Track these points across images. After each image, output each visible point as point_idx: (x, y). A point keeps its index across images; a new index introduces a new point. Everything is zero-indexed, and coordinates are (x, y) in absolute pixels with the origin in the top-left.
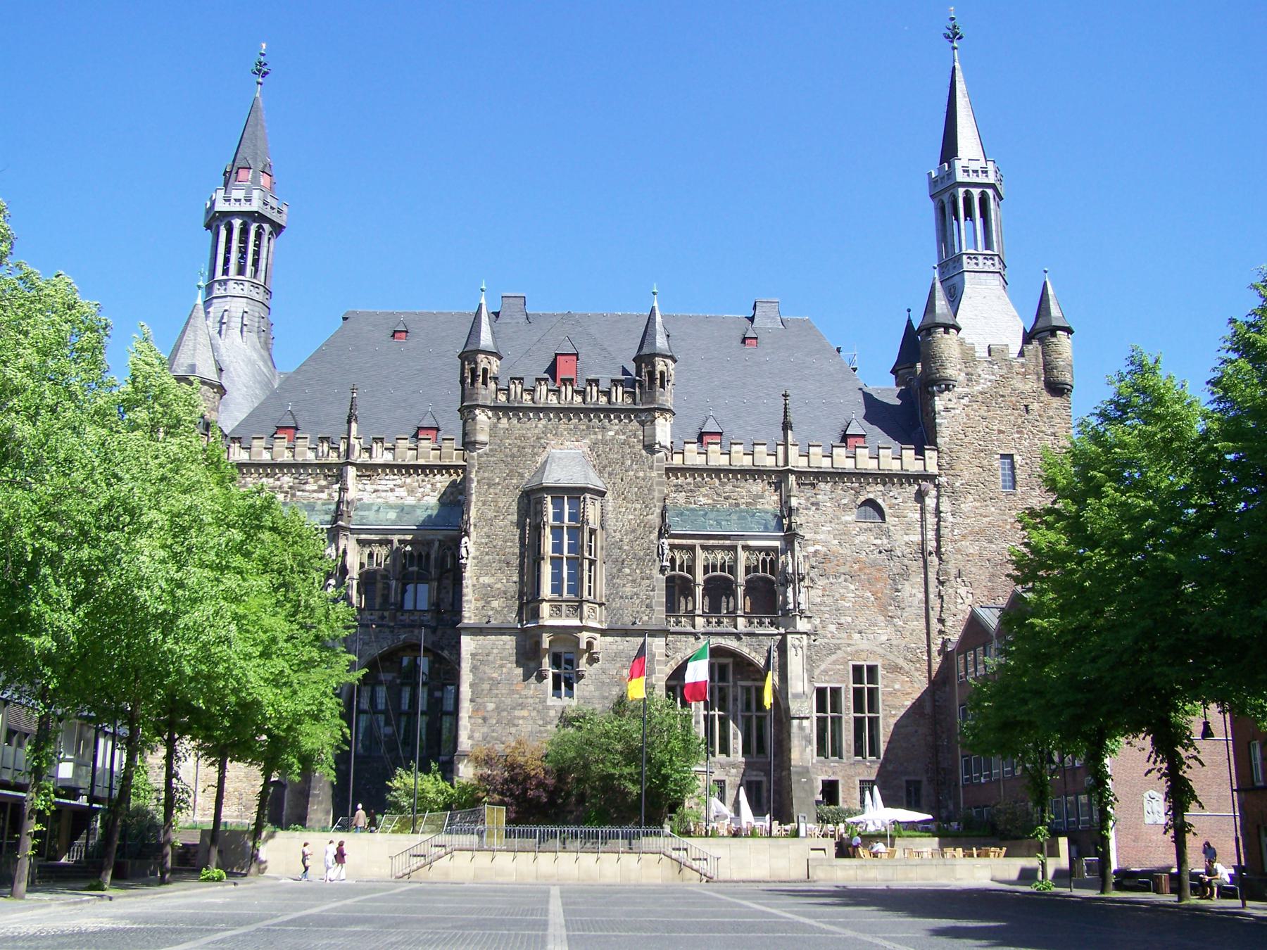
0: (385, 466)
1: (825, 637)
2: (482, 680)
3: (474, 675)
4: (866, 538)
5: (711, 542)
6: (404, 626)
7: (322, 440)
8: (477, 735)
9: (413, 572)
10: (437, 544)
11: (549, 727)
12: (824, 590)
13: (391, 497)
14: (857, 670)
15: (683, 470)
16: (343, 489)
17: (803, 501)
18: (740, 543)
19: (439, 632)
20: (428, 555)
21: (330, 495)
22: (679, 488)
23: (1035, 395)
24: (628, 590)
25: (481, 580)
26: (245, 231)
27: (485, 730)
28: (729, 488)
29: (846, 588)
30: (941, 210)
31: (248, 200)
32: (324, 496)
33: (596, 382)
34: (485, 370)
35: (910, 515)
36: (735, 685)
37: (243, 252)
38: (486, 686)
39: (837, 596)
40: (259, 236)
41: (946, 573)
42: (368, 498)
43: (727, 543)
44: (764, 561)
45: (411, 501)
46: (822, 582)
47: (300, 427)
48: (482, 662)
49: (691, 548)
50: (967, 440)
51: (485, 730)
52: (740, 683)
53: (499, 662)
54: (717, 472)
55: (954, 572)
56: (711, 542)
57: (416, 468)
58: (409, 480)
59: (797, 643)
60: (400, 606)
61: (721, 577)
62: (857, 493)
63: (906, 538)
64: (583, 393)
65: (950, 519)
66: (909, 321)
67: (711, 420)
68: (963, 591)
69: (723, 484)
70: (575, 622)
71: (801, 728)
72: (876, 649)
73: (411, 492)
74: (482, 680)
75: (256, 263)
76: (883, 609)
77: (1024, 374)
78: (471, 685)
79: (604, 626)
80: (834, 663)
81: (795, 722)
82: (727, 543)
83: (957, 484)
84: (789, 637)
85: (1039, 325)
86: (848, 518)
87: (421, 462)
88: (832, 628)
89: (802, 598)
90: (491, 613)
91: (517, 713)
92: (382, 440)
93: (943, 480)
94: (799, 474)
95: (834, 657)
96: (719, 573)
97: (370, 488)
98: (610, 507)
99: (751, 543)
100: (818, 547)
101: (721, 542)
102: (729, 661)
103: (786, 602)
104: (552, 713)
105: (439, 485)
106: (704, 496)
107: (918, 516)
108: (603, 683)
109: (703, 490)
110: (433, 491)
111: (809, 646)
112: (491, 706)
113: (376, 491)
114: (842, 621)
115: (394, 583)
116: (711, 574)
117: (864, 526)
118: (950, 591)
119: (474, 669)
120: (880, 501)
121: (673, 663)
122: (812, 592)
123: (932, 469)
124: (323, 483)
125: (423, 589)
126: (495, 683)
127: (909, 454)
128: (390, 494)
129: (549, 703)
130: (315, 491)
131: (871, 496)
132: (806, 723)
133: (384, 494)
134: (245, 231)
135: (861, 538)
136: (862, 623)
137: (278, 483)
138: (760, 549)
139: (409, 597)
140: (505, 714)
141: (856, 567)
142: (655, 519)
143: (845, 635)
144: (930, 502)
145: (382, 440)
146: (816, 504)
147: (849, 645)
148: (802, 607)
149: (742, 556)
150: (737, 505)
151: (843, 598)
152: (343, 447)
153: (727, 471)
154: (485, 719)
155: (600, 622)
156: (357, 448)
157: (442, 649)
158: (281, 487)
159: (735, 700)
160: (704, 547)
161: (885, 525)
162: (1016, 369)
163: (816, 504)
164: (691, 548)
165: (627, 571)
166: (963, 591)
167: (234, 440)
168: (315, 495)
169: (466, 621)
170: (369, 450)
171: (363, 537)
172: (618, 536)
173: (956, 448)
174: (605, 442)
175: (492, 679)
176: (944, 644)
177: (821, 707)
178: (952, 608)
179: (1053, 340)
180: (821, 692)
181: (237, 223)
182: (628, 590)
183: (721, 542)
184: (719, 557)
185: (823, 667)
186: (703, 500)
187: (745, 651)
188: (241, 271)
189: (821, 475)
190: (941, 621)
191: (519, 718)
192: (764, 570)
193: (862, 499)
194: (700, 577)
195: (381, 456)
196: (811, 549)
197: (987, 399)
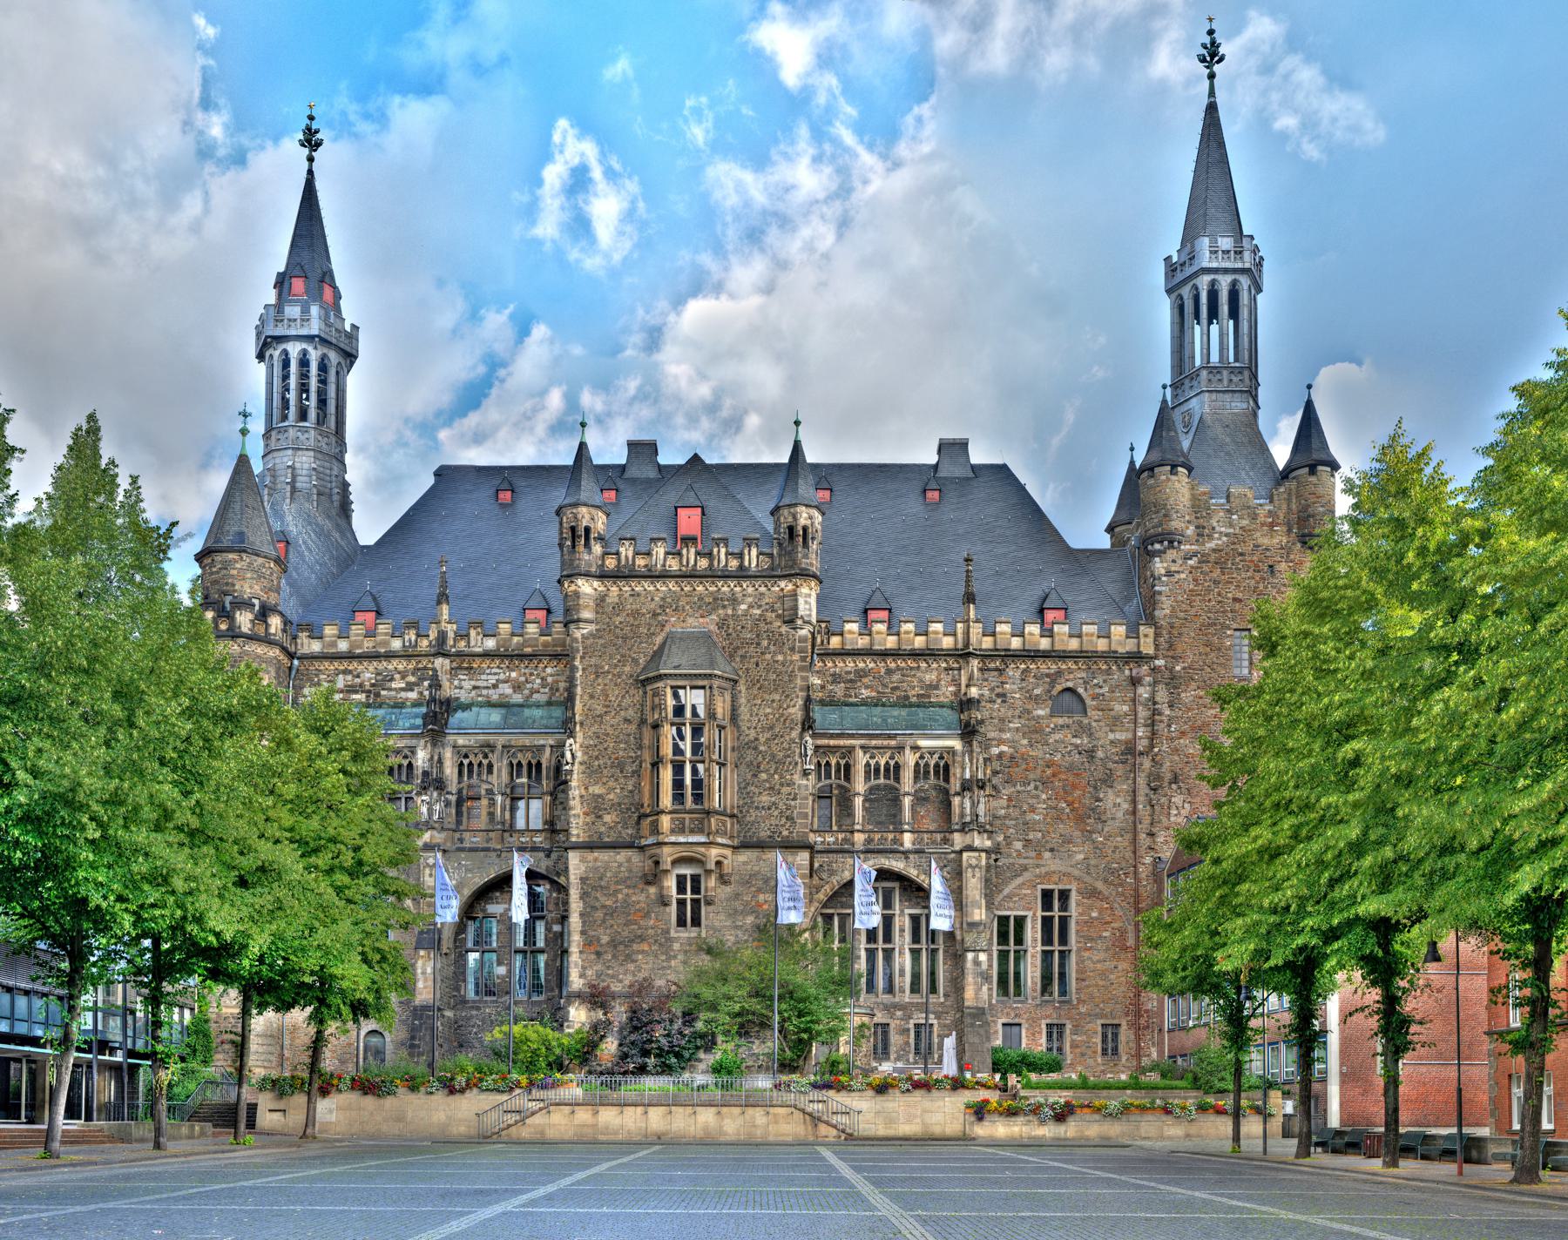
0: (486, 655)
1: (1009, 856)
2: (594, 908)
3: (585, 903)
4: (1063, 739)
5: (874, 742)
7: (413, 625)
8: (589, 972)
9: (522, 785)
10: (548, 750)
11: (673, 963)
12: (1010, 799)
13: (494, 696)
14: (1047, 896)
15: (843, 653)
16: (436, 684)
17: (986, 693)
18: (910, 742)
19: (554, 856)
20: (539, 764)
21: (421, 693)
23: (1286, 551)
25: (591, 790)
27: (599, 967)
28: (896, 677)
29: (1038, 797)
30: (1180, 309)
31: (305, 319)
32: (413, 695)
35: (1117, 707)
36: (902, 911)
38: (599, 915)
39: (1025, 807)
41: (1159, 778)
42: (464, 696)
43: (893, 743)
44: (937, 766)
45: (517, 698)
46: (1006, 791)
47: (384, 611)
48: (594, 888)
49: (851, 750)
50: (1193, 612)
51: (599, 967)
52: (907, 911)
53: (612, 888)
55: (1168, 776)
57: (521, 657)
58: (514, 675)
59: (974, 862)
61: (877, 787)
62: (1053, 683)
63: (1111, 736)
65: (1167, 712)
66: (1132, 463)
67: (878, 594)
68: (1177, 800)
70: (703, 839)
71: (977, 963)
72: (1070, 870)
73: (517, 687)
74: (594, 908)
76: (1080, 819)
77: (1272, 525)
78: (582, 915)
79: (736, 843)
80: (1020, 887)
81: (970, 956)
82: (893, 743)
83: (1178, 668)
84: (965, 855)
85: (1294, 465)
86: (1041, 712)
87: (528, 650)
88: (1018, 845)
89: (981, 809)
90: (603, 829)
91: (635, 947)
92: (481, 624)
93: (1157, 662)
94: (985, 656)
95: (1019, 880)
96: (882, 781)
97: (467, 685)
99: (923, 743)
100: (1004, 748)
101: (886, 743)
102: (896, 885)
103: (962, 815)
104: (676, 946)
105: (550, 679)
106: (867, 687)
107: (1126, 708)
108: (736, 911)
109: (865, 680)
110: (544, 686)
111: (988, 867)
112: (605, 939)
113: (475, 688)
114: (1031, 837)
115: (499, 799)
116: (873, 782)
117: (1060, 721)
118: (1163, 800)
119: (584, 896)
120: (1081, 690)
121: (827, 887)
122: (994, 803)
123: (1148, 649)
124: (412, 679)
125: (536, 805)
126: (611, 912)
127: (1118, 631)
128: (491, 692)
129: (673, 934)
130: (402, 689)
131: (1070, 684)
132: (983, 957)
133: (485, 692)
135: (1057, 736)
136: (1054, 839)
137: (357, 681)
138: (932, 754)
139: (520, 814)
140: (621, 947)
141: (1049, 772)
143: (1033, 854)
144: (1144, 692)
145: (481, 624)
146: (1002, 695)
147: (1038, 866)
148: (982, 819)
150: (907, 698)
151: (1033, 810)
152: (433, 635)
154: (598, 954)
155: (732, 837)
156: (451, 635)
157: (558, 874)
158: (361, 685)
159: (902, 930)
160: (862, 747)
161: (1086, 721)
162: (1261, 519)
163: (1002, 695)
164: (851, 750)
165: (764, 776)
166: (1177, 800)
167: (300, 627)
168: (403, 694)
169: (574, 839)
170: (468, 635)
171: (461, 741)
173: (1177, 623)
175: (604, 906)
176: (1158, 860)
177: (1003, 937)
178: (1164, 820)
179: (1313, 479)
180: (1003, 921)
183: (886, 743)
184: (883, 763)
185: (1006, 891)
186: (865, 693)
187: (913, 873)
189: (1009, 656)
190: (1151, 835)
191: (639, 952)
192: (937, 773)
193: (1059, 688)
194: (860, 785)
196: (995, 751)
197: (1220, 560)
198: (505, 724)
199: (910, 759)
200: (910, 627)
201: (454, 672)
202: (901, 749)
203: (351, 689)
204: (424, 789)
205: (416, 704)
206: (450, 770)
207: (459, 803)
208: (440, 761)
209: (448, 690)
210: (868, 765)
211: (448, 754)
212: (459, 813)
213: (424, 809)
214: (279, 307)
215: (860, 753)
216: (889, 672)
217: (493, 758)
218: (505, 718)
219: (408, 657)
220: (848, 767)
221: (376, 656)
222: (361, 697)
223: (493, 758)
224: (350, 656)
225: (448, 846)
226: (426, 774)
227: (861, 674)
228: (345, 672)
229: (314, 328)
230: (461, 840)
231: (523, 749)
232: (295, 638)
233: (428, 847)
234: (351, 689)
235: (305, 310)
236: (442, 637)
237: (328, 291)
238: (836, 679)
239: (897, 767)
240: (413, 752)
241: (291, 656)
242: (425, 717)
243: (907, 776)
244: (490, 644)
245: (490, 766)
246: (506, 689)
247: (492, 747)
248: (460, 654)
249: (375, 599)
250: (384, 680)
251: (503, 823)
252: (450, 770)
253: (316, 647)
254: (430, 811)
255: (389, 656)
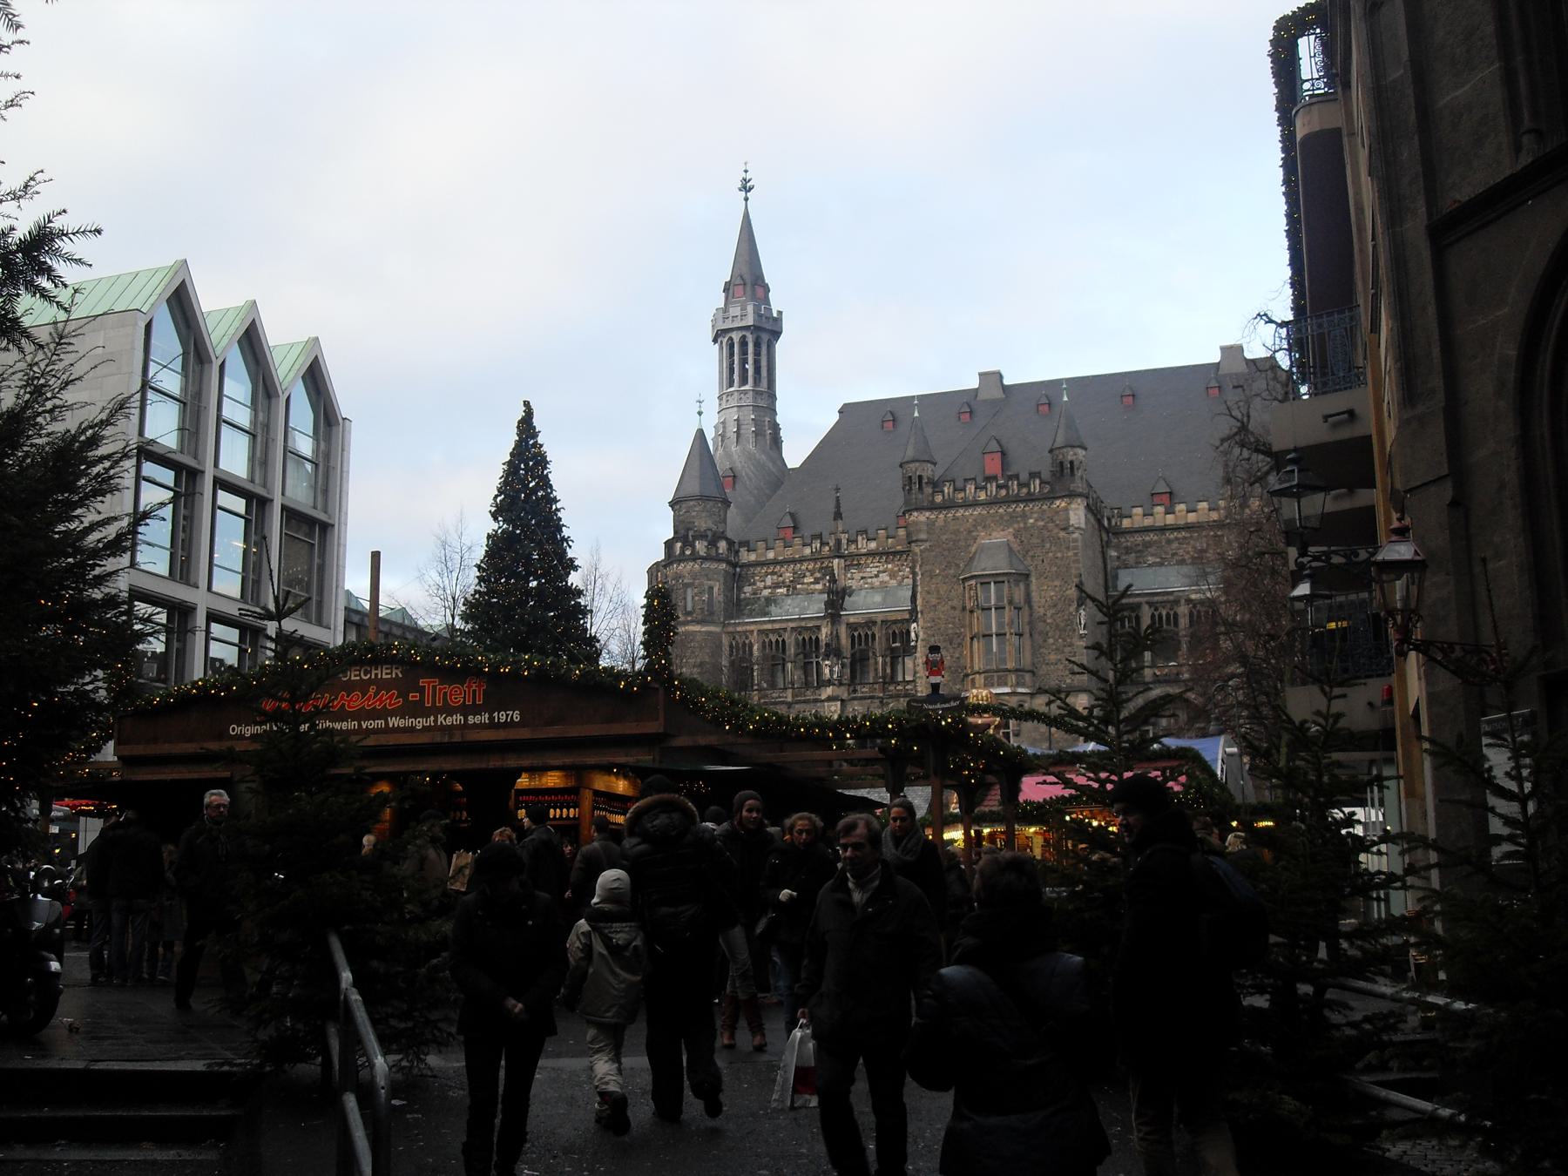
0: (871, 554)
5: (1156, 599)
6: (891, 697)
7: (814, 537)
16: (833, 580)
22: (1128, 551)
24: (1053, 657)
26: (743, 343)
28: (1175, 545)
32: (819, 587)
33: (1017, 477)
34: (920, 477)
37: (744, 361)
40: (757, 345)
42: (853, 584)
49: (1139, 605)
54: (1163, 529)
56: (1156, 599)
57: (895, 553)
60: (893, 679)
64: (1005, 486)
69: (1169, 542)
73: (893, 575)
75: (757, 370)
92: (865, 532)
97: (858, 576)
98: (1033, 587)
99: (1193, 597)
134: (743, 343)
142: (1072, 592)
149: (1183, 610)
153: (1177, 528)
156: (844, 542)
160: (1150, 604)
164: (1139, 605)
167: (742, 544)
170: (856, 541)
171: (852, 620)
172: (1042, 610)
174: (1026, 529)
181: (736, 337)
182: (1053, 657)
186: (1151, 560)
188: (744, 381)
195: (864, 545)
198: (884, 603)
199: (1183, 610)
200: (1182, 507)
201: (847, 568)
202: (1177, 602)
203: (776, 586)
204: (827, 657)
205: (821, 592)
206: (845, 641)
207: (853, 664)
208: (838, 636)
209: (842, 583)
210: (1153, 616)
211: (843, 630)
212: (853, 672)
213: (827, 671)
214: (725, 310)
215: (1146, 608)
216: (1169, 542)
217: (876, 630)
218: (884, 599)
219: (815, 560)
220: (1138, 618)
221: (794, 561)
222: (783, 590)
223: (876, 630)
224: (775, 562)
225: (845, 696)
226: (827, 645)
227: (1147, 545)
228: (773, 573)
229: (750, 321)
230: (855, 691)
231: (895, 622)
232: (737, 552)
233: (830, 699)
234: (776, 586)
235: (744, 308)
236: (839, 542)
237: (760, 291)
238: (1128, 551)
239: (1176, 615)
240: (819, 628)
241: (735, 565)
242: (826, 604)
243: (1184, 622)
244: (873, 545)
245: (873, 636)
246: (884, 577)
247: (875, 623)
248: (851, 555)
249: (792, 515)
250: (798, 578)
251: (884, 677)
252: (845, 641)
253: (753, 557)
254: (831, 672)
255: (801, 560)
